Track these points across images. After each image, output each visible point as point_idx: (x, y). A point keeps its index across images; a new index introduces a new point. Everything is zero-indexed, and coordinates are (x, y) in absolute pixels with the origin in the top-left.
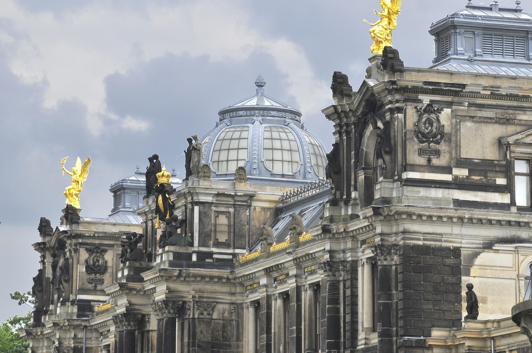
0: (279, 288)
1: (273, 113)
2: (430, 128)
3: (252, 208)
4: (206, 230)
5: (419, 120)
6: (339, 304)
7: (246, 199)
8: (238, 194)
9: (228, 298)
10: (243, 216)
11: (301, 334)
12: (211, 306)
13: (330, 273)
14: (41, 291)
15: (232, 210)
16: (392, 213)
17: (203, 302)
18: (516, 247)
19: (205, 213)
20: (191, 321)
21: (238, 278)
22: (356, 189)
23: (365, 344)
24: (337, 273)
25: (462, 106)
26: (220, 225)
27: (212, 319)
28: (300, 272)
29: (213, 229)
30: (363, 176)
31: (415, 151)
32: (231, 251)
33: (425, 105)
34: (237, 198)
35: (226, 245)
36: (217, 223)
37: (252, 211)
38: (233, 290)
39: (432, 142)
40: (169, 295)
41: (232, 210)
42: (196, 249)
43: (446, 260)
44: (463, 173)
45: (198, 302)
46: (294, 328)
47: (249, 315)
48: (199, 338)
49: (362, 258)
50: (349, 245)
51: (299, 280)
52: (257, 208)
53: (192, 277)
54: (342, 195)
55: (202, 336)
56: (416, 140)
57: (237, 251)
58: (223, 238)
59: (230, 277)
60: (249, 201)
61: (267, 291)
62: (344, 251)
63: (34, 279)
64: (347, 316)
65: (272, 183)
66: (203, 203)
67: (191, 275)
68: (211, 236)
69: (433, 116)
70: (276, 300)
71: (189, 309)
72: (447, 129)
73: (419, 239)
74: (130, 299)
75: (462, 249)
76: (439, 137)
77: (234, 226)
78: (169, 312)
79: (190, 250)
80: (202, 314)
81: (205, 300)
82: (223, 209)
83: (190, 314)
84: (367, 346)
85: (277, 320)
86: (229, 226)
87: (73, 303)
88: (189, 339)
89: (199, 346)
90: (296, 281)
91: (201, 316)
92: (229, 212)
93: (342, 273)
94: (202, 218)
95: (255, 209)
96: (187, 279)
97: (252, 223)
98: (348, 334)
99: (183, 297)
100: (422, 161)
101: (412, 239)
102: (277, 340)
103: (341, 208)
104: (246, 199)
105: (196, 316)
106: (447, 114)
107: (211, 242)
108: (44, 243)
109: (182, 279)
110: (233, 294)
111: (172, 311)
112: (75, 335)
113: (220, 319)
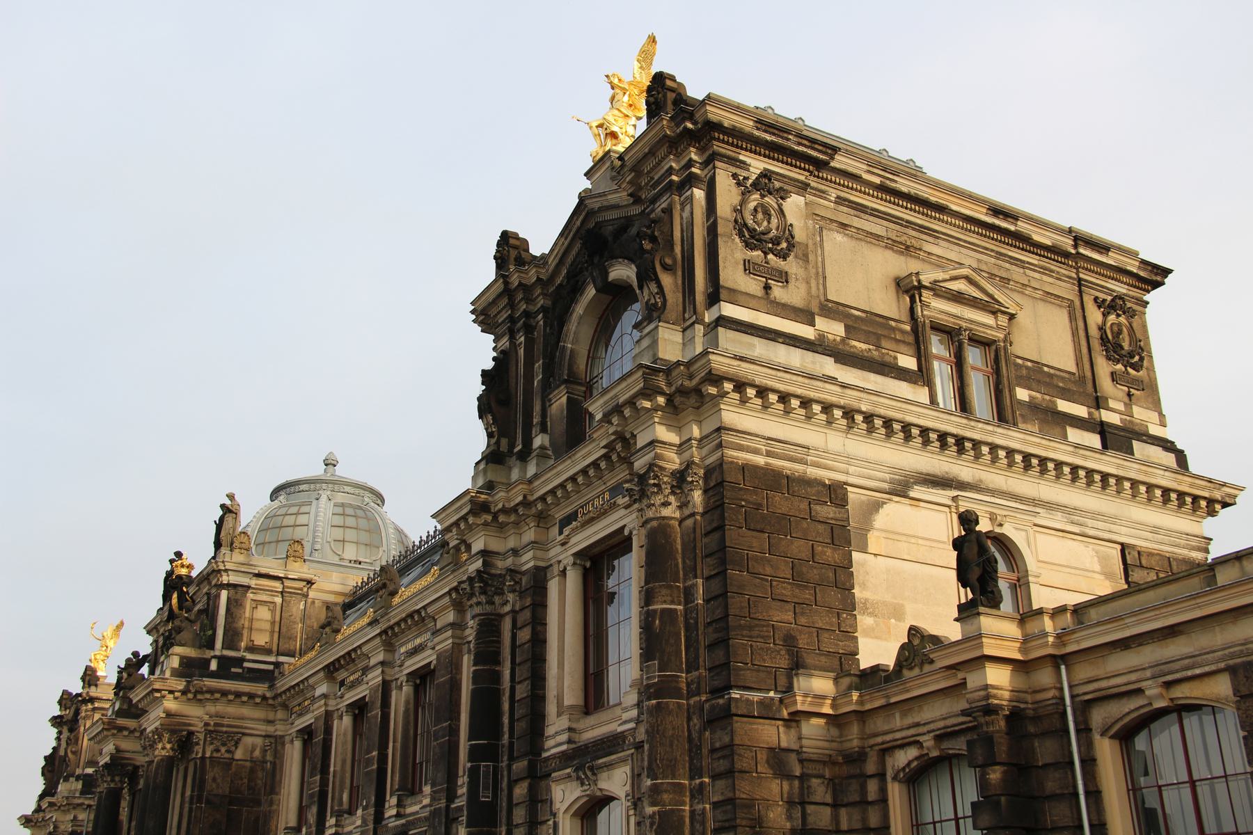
0: (347, 696)
1: (347, 489)
2: (765, 223)
3: (309, 601)
5: (743, 202)
6: (498, 663)
9: (263, 728)
10: (294, 610)
13: (483, 599)
16: (694, 382)
18: (955, 499)
19: (236, 601)
21: (280, 695)
22: (544, 430)
23: (570, 741)
24: (497, 599)
25: (825, 199)
28: (389, 657)
30: (564, 399)
31: (737, 263)
32: (272, 659)
33: (754, 177)
34: (287, 583)
38: (271, 716)
39: (771, 251)
41: (278, 600)
42: (218, 653)
43: (818, 508)
44: (835, 329)
45: (213, 732)
46: (375, 753)
47: (293, 754)
49: (560, 558)
50: (529, 535)
51: (387, 670)
53: (207, 692)
54: (512, 445)
56: (737, 240)
57: (281, 659)
58: (261, 640)
59: (268, 695)
61: (326, 704)
62: (515, 552)
63: (46, 758)
64: (518, 687)
66: (235, 586)
69: (770, 200)
70: (341, 717)
72: (799, 235)
73: (756, 452)
74: (118, 743)
75: (849, 489)
76: (784, 245)
79: (212, 653)
80: (218, 750)
82: (264, 597)
84: (573, 746)
85: (340, 750)
86: (273, 623)
87: (78, 778)
88: (193, 791)
89: (208, 802)
91: (215, 755)
93: (511, 597)
96: (199, 697)
98: (521, 726)
99: (190, 725)
100: (752, 285)
101: (741, 448)
102: (337, 783)
103: (510, 468)
105: (208, 755)
106: (797, 206)
109: (190, 696)
112: (75, 817)
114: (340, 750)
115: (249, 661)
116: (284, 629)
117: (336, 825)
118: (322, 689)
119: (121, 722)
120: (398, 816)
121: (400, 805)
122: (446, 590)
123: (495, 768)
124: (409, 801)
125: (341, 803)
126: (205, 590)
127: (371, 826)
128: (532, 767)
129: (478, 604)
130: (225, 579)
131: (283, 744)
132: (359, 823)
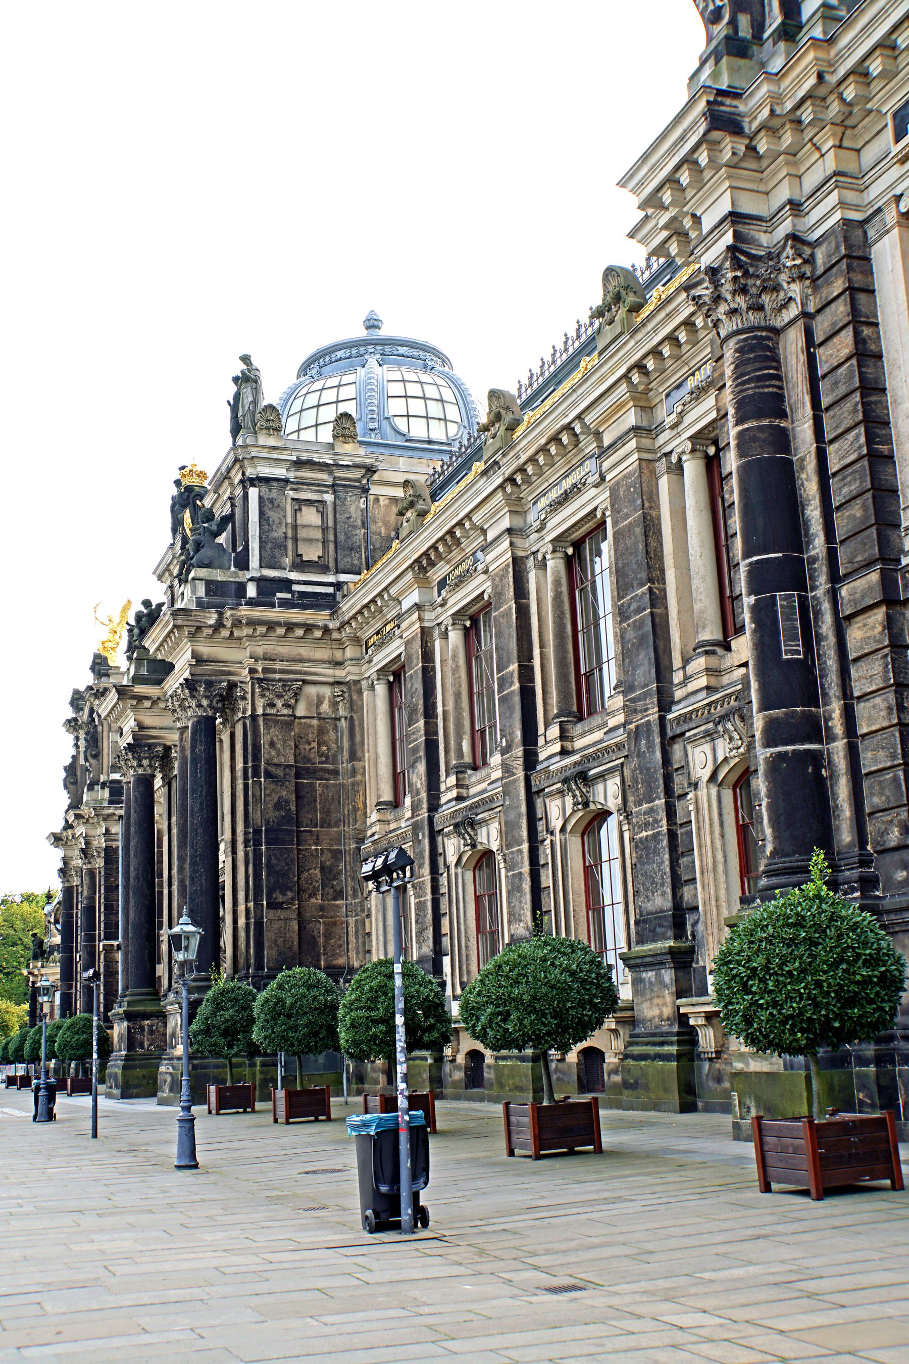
1: (402, 350)
3: (371, 498)
4: (275, 534)
7: (357, 474)
8: (341, 463)
9: (329, 673)
10: (352, 509)
11: (532, 680)
12: (293, 688)
13: (741, 302)
14: (75, 783)
15: (329, 498)
17: (274, 680)
20: (248, 722)
21: (348, 623)
24: (766, 299)
26: (304, 526)
27: (295, 717)
28: (518, 522)
29: (290, 534)
32: (331, 579)
35: (320, 566)
36: (299, 522)
37: (371, 503)
38: (338, 655)
40: (199, 669)
41: (329, 498)
48: (267, 756)
51: (518, 541)
52: (381, 498)
54: (758, 27)
55: (273, 753)
57: (343, 577)
58: (311, 553)
60: (364, 481)
61: (420, 619)
63: (65, 768)
64: (831, 449)
65: (410, 453)
67: (244, 621)
68: (286, 547)
70: (445, 636)
71: (244, 698)
74: (140, 718)
77: (335, 529)
78: (199, 706)
80: (273, 705)
81: (277, 676)
83: (245, 707)
85: (449, 681)
86: (324, 529)
87: (104, 785)
88: (245, 762)
89: (268, 775)
90: (511, 544)
91: (269, 711)
92: (323, 502)
93: (795, 290)
94: (266, 509)
95: (377, 500)
97: (373, 527)
99: (230, 673)
104: (357, 474)
105: (260, 711)
107: (288, 561)
108: (75, 720)
109: (225, 633)
110: (338, 664)
111: (205, 703)
112: (107, 830)
113: (313, 718)
114: (449, 681)
115: (299, 583)
116: (341, 537)
117: (458, 786)
118: (414, 597)
119: (139, 689)
120: (564, 752)
121: (563, 736)
122: (623, 370)
123: (803, 601)
124: (579, 728)
125: (460, 754)
126: (227, 494)
127: (520, 774)
128: (888, 582)
129: (734, 312)
130: (250, 472)
131: (360, 692)
132: (498, 774)
